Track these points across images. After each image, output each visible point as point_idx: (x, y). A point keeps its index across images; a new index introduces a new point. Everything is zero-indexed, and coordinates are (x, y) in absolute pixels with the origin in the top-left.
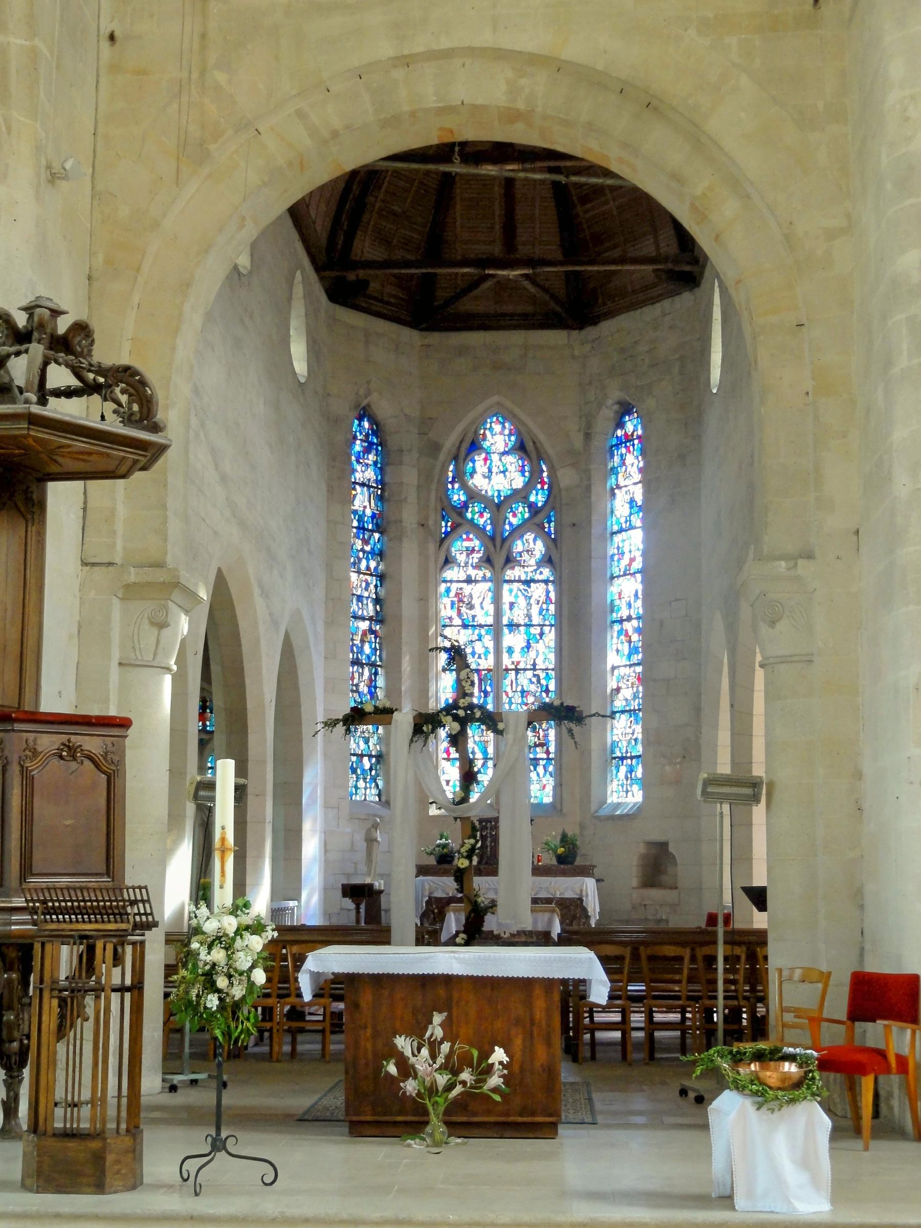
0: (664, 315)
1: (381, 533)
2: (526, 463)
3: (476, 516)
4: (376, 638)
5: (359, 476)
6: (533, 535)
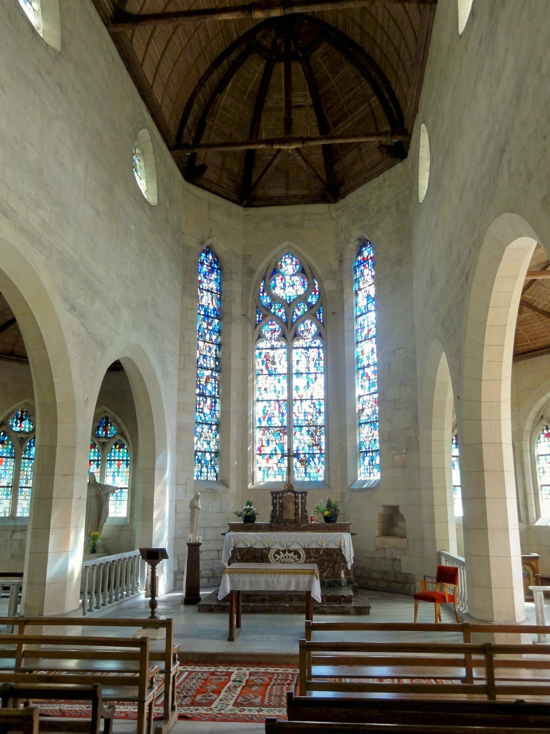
0: (385, 180)
1: (219, 320)
2: (305, 280)
3: (277, 311)
4: (215, 381)
5: (205, 285)
6: (310, 321)
